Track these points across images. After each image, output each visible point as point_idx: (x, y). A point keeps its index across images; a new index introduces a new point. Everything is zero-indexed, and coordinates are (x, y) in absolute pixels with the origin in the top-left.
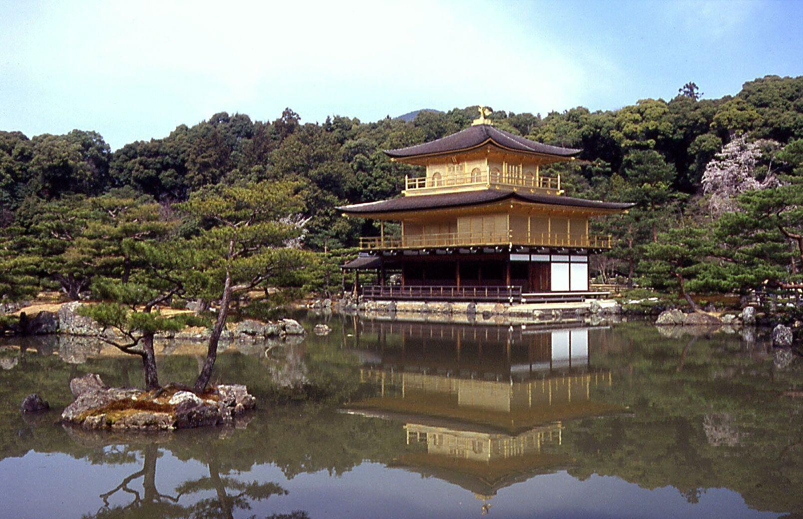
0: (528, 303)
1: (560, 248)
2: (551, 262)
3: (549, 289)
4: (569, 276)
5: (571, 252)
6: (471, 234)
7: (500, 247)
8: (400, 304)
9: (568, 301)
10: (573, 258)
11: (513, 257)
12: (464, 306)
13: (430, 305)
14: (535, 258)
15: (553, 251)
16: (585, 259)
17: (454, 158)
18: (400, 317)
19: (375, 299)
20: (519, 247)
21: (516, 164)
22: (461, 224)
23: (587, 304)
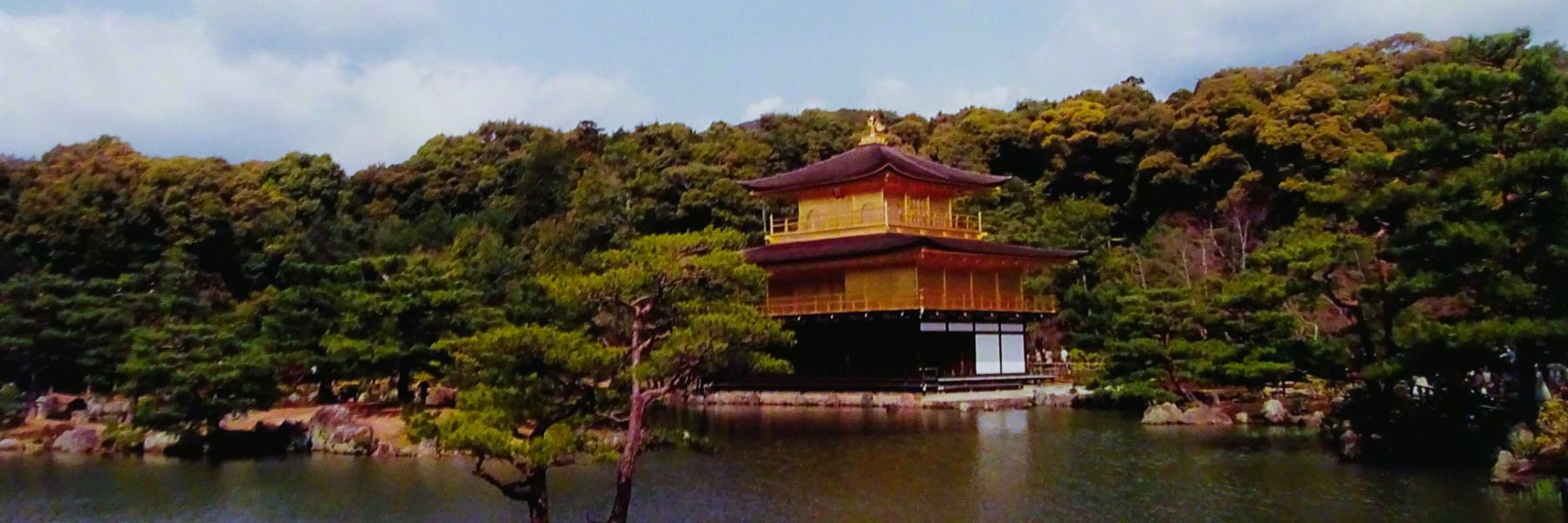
0: (947, 391)
1: (988, 313)
2: (974, 333)
3: (975, 374)
4: (999, 354)
5: (1002, 318)
6: (865, 295)
7: (906, 312)
8: (766, 396)
9: (1001, 389)
10: (1004, 327)
11: (924, 327)
12: (857, 398)
13: (809, 397)
14: (953, 327)
15: (977, 317)
16: (1020, 328)
17: (837, 190)
18: (766, 410)
19: (729, 389)
20: (933, 312)
21: (923, 198)
22: (851, 283)
23: (1027, 392)
